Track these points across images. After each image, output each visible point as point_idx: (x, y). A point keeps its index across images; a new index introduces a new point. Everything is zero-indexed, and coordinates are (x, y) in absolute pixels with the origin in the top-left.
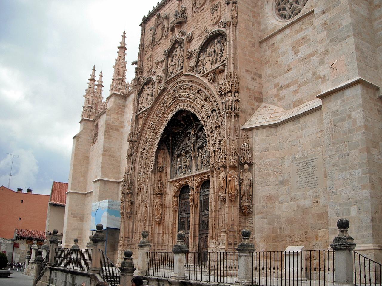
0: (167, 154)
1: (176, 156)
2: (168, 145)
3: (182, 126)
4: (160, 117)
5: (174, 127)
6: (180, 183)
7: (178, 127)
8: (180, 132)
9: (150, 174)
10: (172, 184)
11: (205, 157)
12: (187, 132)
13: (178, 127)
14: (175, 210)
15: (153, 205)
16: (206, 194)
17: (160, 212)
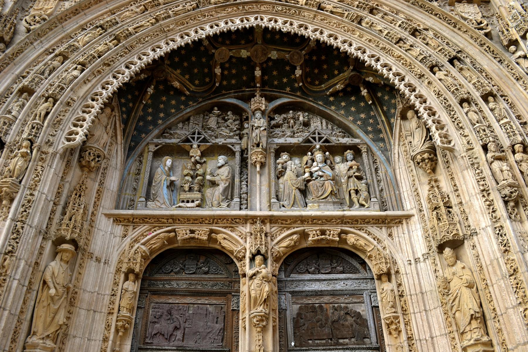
0: (115, 128)
1: (152, 148)
2: (124, 109)
3: (197, 82)
4: (169, 17)
5: (176, 70)
6: (174, 231)
7: (187, 77)
8: (185, 95)
9: (54, 154)
10: (119, 229)
11: (321, 176)
12: (215, 100)
13: (187, 77)
14: (122, 330)
15: (30, 282)
16: (307, 288)
17: (61, 318)
